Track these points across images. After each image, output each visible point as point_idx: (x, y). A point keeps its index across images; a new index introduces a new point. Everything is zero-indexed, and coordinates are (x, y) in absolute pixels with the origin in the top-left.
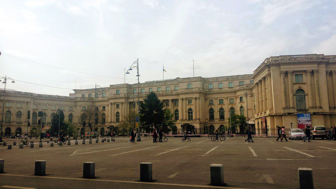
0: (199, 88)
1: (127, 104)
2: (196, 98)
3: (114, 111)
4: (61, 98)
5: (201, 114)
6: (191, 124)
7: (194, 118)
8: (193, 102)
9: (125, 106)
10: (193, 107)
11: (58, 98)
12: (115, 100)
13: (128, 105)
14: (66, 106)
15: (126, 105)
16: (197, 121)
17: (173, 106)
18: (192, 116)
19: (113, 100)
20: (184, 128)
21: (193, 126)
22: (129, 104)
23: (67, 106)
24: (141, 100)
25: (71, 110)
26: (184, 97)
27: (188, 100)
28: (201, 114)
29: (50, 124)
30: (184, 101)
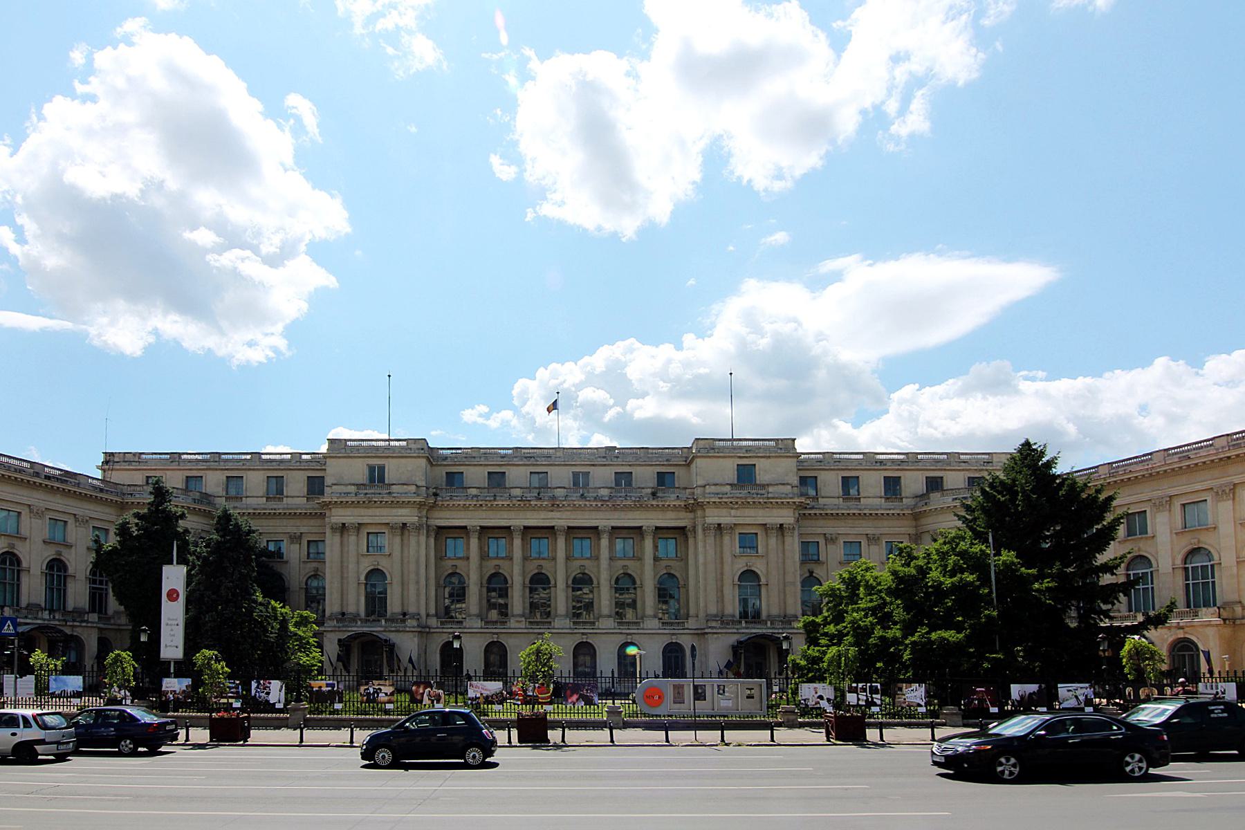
1: (428, 537)
4: (48, 477)
9: (418, 543)
12: (363, 511)
13: (432, 541)
14: (76, 520)
15: (423, 539)
19: (348, 511)
22: (433, 534)
23: (79, 520)
24: (129, 516)
25: (59, 537)
26: (725, 517)
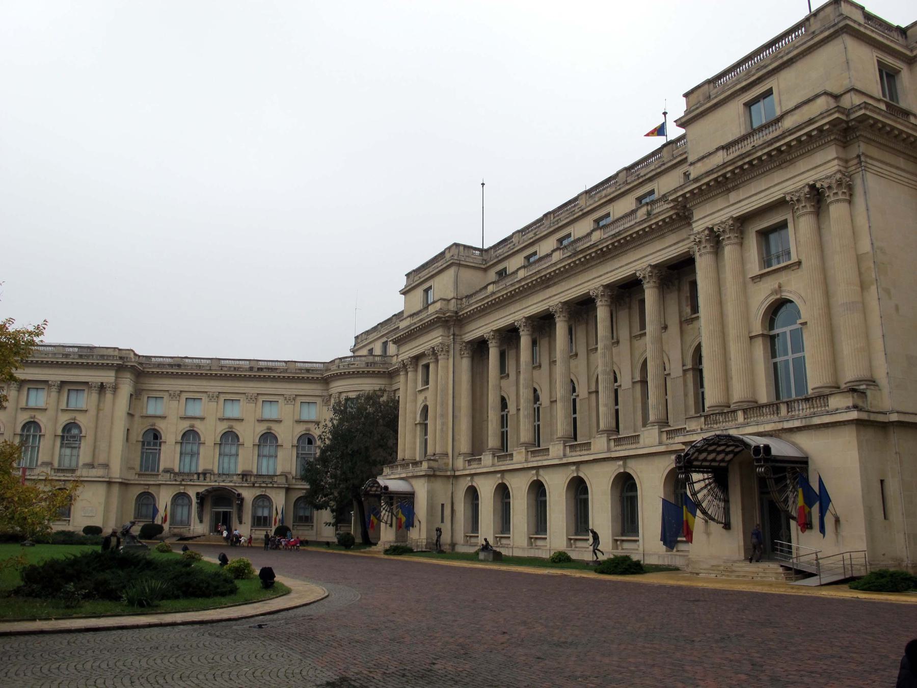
0: (836, 97)
2: (817, 196)
3: (415, 401)
5: (876, 333)
6: (779, 448)
7: (815, 379)
8: (800, 232)
10: (796, 286)
11: (251, 369)
16: (836, 402)
17: (681, 323)
18: (800, 364)
20: (720, 479)
21: (798, 467)
27: (764, 234)
28: (876, 333)
29: (202, 478)
30: (729, 251)
